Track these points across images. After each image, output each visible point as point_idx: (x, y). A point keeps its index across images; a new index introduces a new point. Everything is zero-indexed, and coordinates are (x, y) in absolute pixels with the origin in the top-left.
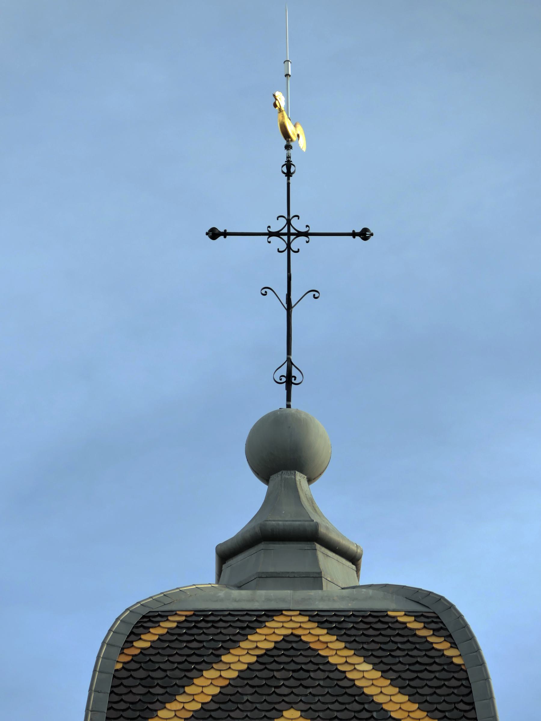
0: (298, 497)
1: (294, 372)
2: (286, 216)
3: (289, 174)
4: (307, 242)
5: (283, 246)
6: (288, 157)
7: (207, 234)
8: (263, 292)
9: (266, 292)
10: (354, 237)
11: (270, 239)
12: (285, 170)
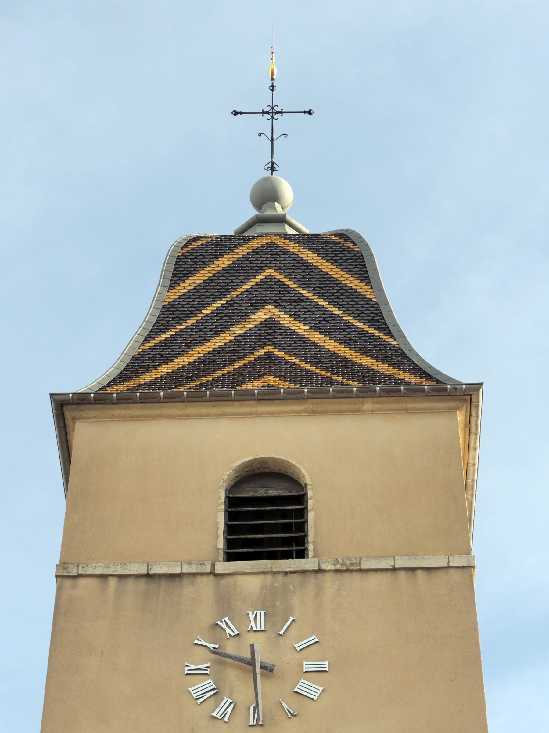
0: (277, 211)
1: (275, 166)
2: (271, 106)
3: (273, 90)
4: (282, 116)
5: (269, 117)
6: (273, 83)
7: (232, 113)
8: (260, 135)
9: (261, 135)
10: (305, 114)
11: (263, 115)
12: (271, 88)
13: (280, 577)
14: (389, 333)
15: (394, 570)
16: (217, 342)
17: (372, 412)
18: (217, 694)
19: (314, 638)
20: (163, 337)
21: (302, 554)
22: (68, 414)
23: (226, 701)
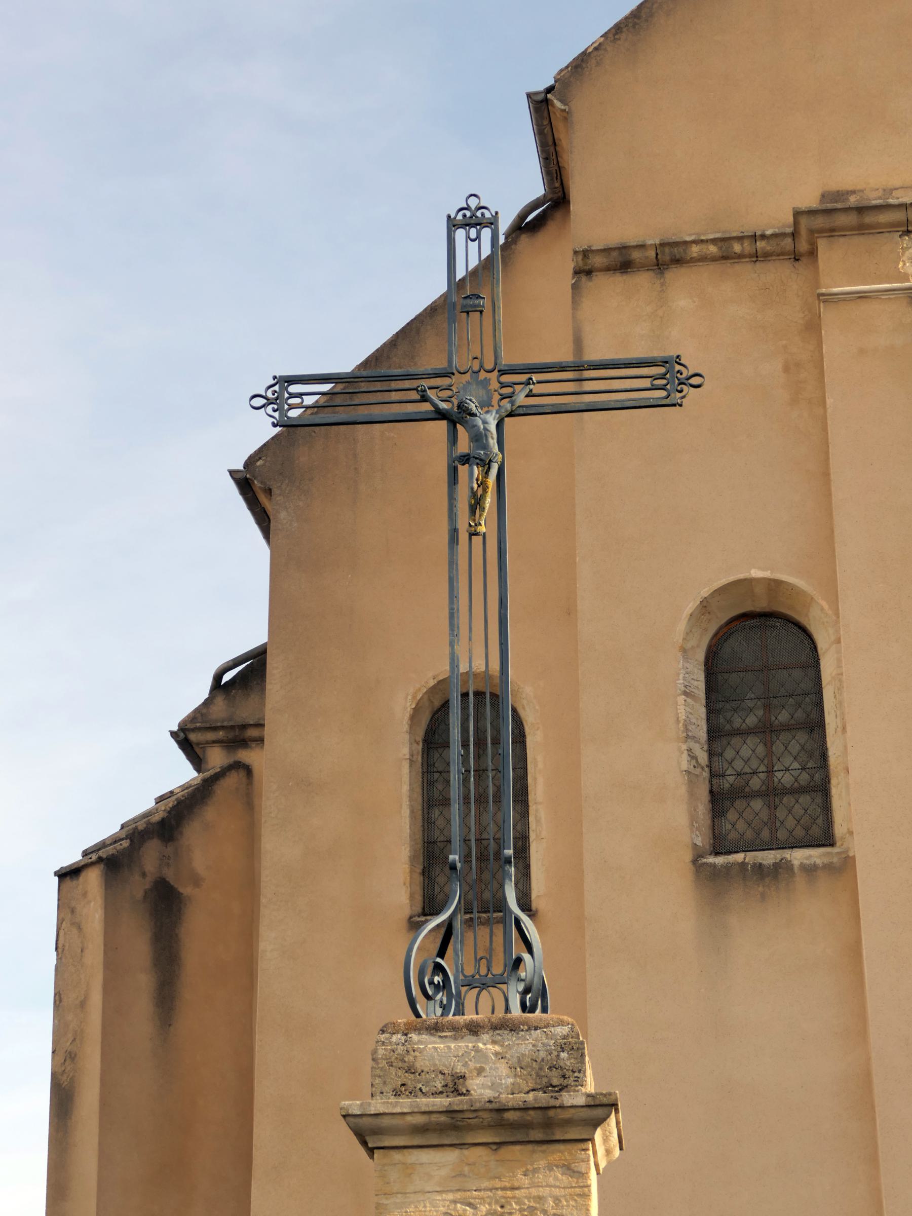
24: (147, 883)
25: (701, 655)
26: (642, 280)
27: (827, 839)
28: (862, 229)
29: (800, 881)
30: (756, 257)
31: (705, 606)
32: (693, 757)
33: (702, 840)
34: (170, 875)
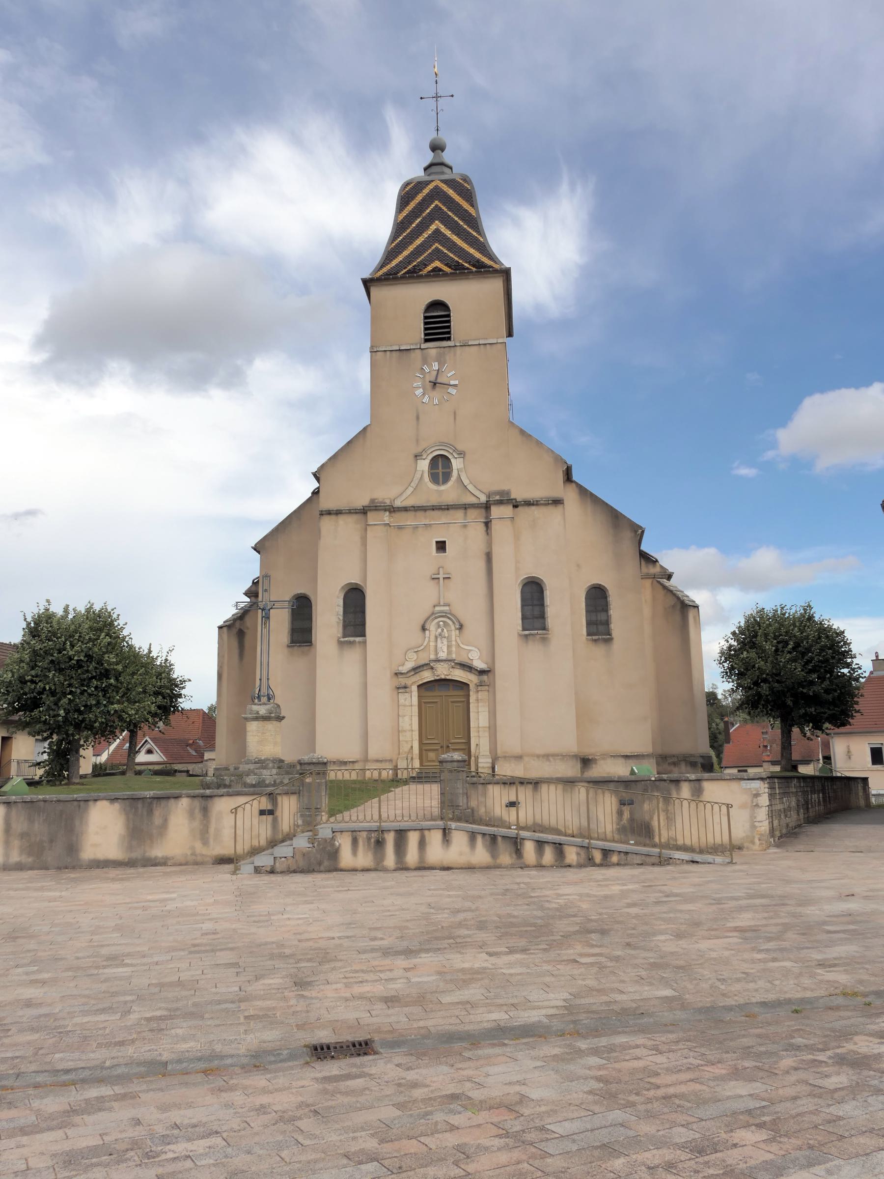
13: (442, 349)
14: (479, 234)
15: (479, 344)
16: (418, 242)
17: (472, 278)
18: (424, 394)
19: (454, 372)
20: (399, 239)
21: (449, 339)
22: (368, 285)
23: (427, 396)
24: (237, 630)
25: (342, 597)
26: (333, 517)
27: (363, 635)
28: (376, 510)
29: (357, 644)
30: (356, 513)
31: (343, 588)
32: (339, 619)
33: (340, 635)
34: (242, 628)
